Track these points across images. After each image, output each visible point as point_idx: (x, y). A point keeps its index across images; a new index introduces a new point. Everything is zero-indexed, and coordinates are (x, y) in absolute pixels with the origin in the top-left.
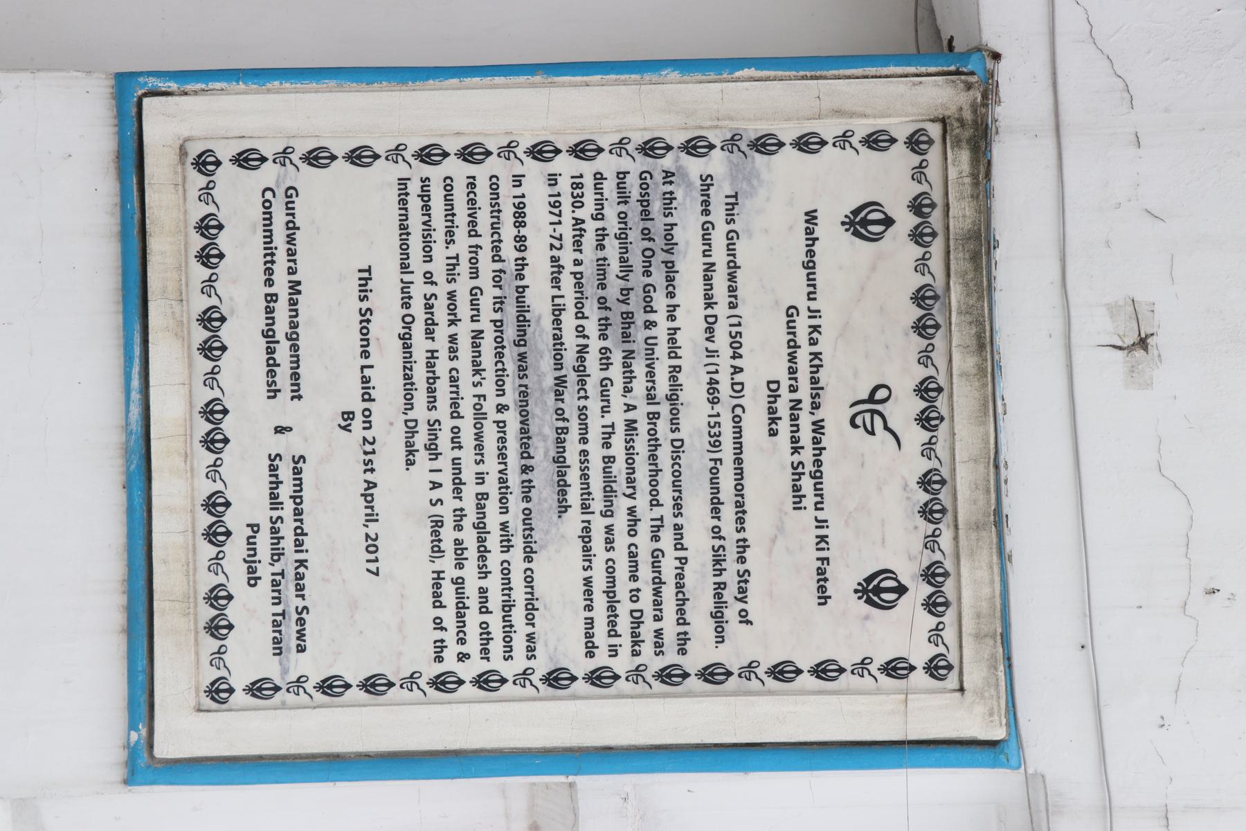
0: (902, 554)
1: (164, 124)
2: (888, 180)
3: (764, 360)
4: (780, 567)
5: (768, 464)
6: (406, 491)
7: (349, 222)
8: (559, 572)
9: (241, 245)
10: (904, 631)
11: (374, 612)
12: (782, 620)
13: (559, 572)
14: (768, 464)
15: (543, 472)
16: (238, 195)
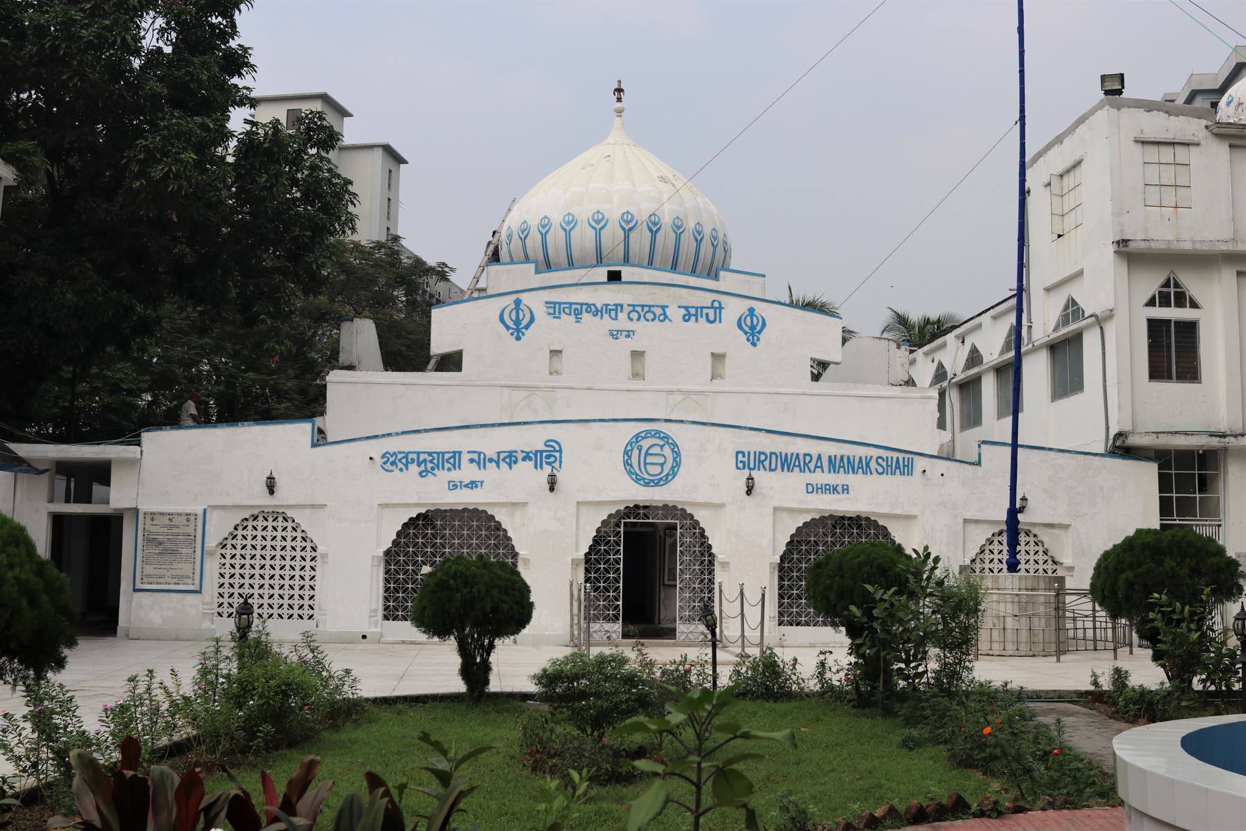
0: (184, 518)
1: (139, 586)
2: (148, 517)
3: (165, 530)
4: (186, 530)
5: (175, 530)
6: (175, 565)
7: (149, 569)
8: (184, 551)
9: (150, 580)
10: (192, 518)
11: (185, 568)
12: (190, 530)
13: (184, 551)
14: (175, 530)
15: (174, 552)
16: (145, 580)
